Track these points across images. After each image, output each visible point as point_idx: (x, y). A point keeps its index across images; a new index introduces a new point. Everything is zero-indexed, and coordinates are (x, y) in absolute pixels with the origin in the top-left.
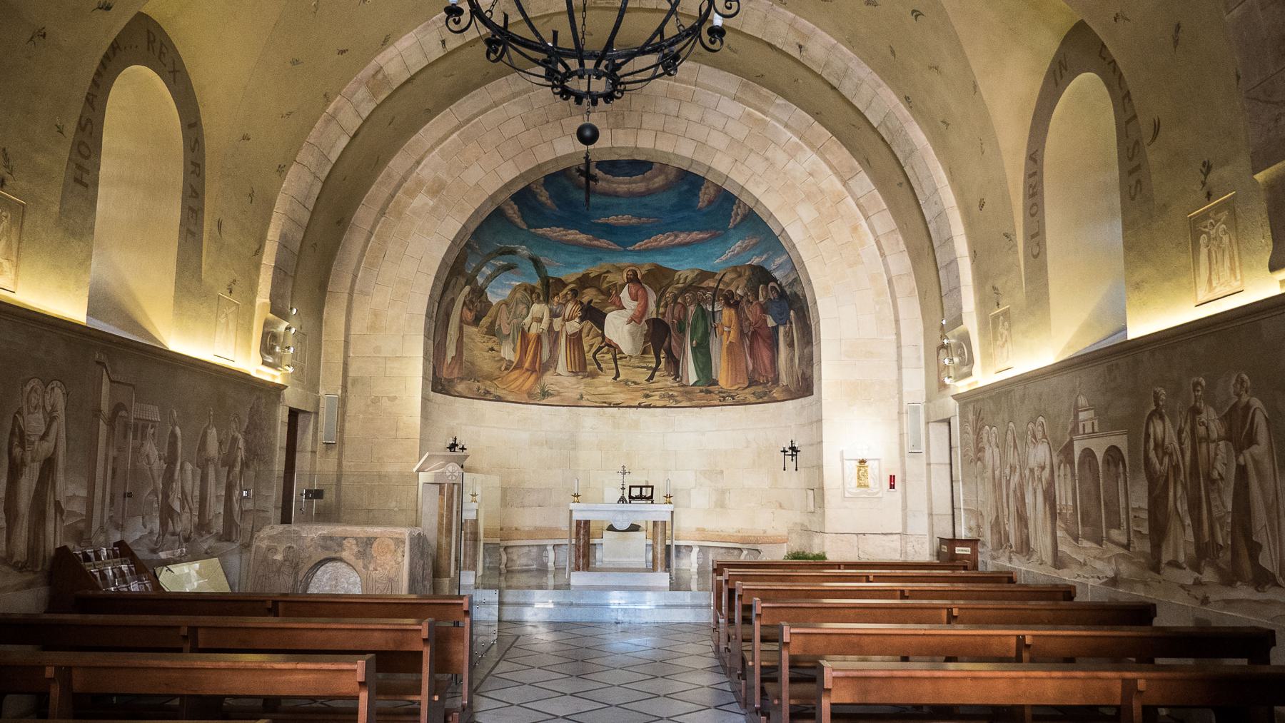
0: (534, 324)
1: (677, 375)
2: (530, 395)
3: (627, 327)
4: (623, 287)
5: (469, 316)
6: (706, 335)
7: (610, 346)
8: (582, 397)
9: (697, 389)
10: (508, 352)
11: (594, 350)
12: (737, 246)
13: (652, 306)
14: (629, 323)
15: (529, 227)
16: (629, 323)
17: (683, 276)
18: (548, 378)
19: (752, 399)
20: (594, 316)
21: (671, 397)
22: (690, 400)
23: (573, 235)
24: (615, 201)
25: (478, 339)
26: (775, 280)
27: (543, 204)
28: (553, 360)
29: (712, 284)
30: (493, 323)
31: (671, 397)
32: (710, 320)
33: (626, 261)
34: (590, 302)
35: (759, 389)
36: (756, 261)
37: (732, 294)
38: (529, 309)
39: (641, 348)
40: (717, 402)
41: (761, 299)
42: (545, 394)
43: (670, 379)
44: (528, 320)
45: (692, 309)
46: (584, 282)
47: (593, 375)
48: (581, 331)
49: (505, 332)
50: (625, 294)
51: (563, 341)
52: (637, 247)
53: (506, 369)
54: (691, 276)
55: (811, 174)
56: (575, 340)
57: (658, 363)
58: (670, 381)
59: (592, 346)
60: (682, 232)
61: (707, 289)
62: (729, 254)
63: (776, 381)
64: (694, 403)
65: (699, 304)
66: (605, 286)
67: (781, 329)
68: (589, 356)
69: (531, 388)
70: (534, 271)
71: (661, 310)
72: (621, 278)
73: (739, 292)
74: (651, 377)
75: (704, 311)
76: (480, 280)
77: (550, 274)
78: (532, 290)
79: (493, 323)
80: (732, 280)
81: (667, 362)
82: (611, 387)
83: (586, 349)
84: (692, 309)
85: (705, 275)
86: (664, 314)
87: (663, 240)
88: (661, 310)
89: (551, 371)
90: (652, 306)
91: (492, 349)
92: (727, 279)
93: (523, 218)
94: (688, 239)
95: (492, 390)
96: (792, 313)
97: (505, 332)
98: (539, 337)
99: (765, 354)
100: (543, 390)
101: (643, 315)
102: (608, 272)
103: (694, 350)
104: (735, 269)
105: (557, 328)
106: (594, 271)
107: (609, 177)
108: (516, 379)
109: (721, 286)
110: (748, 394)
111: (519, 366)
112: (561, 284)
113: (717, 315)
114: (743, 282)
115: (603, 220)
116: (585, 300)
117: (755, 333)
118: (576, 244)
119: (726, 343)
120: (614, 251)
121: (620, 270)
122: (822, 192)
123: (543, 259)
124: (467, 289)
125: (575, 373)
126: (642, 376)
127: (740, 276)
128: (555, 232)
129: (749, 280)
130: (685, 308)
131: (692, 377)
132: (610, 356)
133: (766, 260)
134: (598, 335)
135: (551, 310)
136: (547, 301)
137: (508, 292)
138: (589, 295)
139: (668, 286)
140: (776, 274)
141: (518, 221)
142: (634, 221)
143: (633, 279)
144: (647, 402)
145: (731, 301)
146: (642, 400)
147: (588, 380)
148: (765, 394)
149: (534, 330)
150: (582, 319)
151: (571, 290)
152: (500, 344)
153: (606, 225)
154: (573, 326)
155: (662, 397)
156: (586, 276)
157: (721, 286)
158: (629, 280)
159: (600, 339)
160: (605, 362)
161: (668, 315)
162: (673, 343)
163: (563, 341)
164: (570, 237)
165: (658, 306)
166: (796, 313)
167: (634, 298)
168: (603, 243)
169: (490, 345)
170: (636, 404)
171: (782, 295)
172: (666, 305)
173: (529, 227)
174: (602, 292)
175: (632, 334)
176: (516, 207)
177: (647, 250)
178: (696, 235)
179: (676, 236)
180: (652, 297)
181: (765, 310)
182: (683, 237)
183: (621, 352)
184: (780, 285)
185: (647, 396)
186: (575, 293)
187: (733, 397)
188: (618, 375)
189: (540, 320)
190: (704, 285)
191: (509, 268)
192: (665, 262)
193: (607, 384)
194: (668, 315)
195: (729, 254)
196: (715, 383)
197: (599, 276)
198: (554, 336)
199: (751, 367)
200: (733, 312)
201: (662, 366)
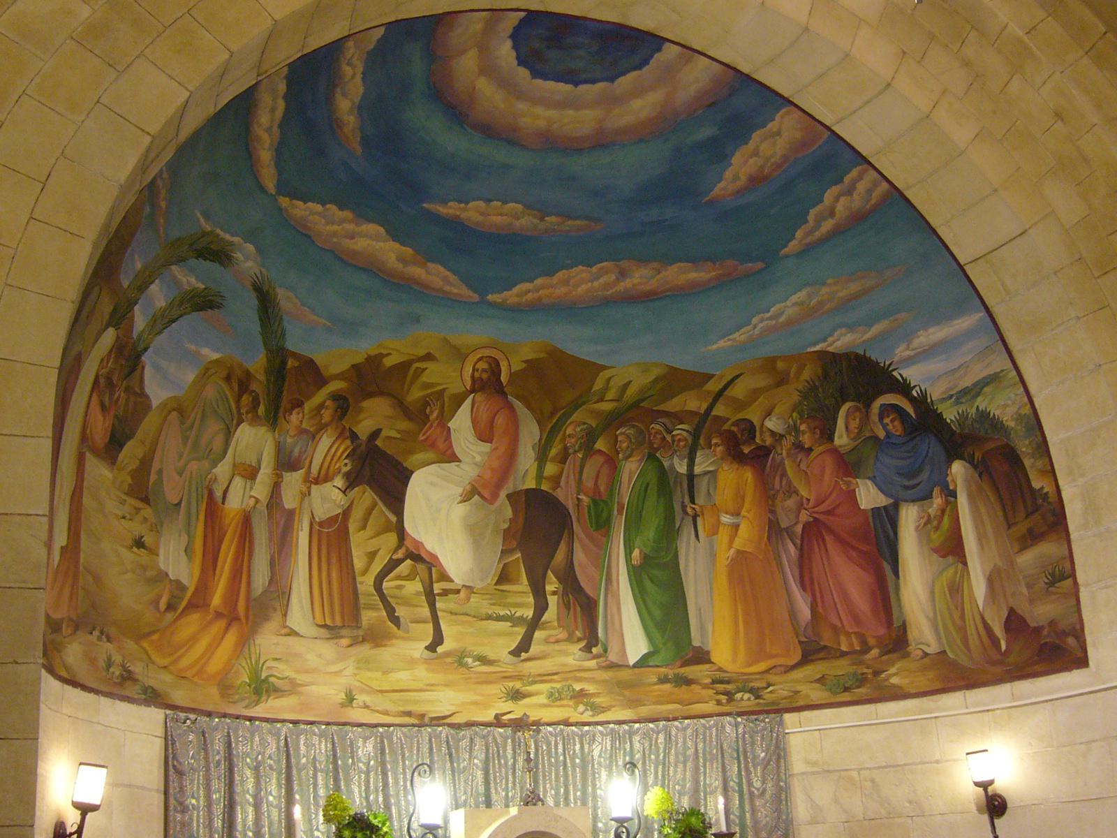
0: (238, 482)
1: (591, 640)
2: (226, 689)
3: (460, 510)
4: (458, 401)
5: (101, 427)
6: (669, 532)
7: (416, 557)
8: (350, 699)
9: (651, 676)
10: (176, 560)
11: (377, 567)
12: (788, 304)
13: (527, 459)
14: (466, 498)
15: (285, 188)
16: (466, 498)
17: (616, 383)
18: (268, 641)
19: (816, 693)
20: (382, 475)
21: (580, 696)
22: (633, 703)
23: (373, 241)
24: (500, 154)
25: (112, 506)
26: (904, 388)
27: (334, 124)
28: (279, 593)
29: (693, 402)
30: (145, 464)
31: (580, 696)
32: (680, 495)
33: (476, 334)
34: (376, 434)
35: (841, 668)
36: (842, 341)
37: (750, 429)
38: (229, 435)
39: (494, 570)
40: (710, 707)
41: (841, 439)
42: (262, 688)
43: (575, 649)
44: (223, 469)
45: (631, 468)
46: (371, 378)
47: (375, 638)
48: (346, 513)
49: (172, 497)
50: (461, 423)
51: (302, 538)
52: (511, 296)
53: (171, 607)
54: (640, 381)
55: (1058, 116)
56: (333, 537)
57: (541, 608)
58: (572, 656)
59: (372, 555)
60: (642, 260)
61: (678, 417)
62: (759, 323)
63: (897, 642)
64: (644, 711)
65: (652, 457)
66: (415, 394)
67: (909, 517)
68: (366, 584)
69: (227, 669)
70: (256, 328)
71: (550, 469)
72: (445, 376)
73: (772, 424)
74: (523, 647)
75: (663, 473)
76: (140, 321)
77: (291, 345)
78: (242, 383)
79: (145, 464)
80: (755, 394)
81: (566, 605)
82: (423, 674)
83: (358, 564)
84: (631, 468)
85: (676, 380)
86: (556, 480)
87: (583, 281)
88: (550, 469)
89: (273, 625)
90: (527, 459)
91: (139, 543)
92: (738, 391)
93: (279, 152)
94: (653, 284)
95: (137, 668)
96: (958, 469)
97: (172, 497)
98: (246, 521)
99: (849, 578)
100: (255, 673)
101: (499, 485)
102: (428, 357)
103: (637, 575)
104: (769, 364)
105: (289, 500)
106: (396, 350)
107: (523, 73)
108: (194, 639)
109: (720, 410)
110: (803, 681)
111: (199, 602)
112: (313, 374)
113: (702, 486)
114: (789, 397)
115: (450, 209)
116: (364, 428)
117: (814, 531)
118: (371, 268)
119: (725, 556)
120: (451, 302)
121: (460, 355)
122: (1085, 160)
123: (285, 299)
124: (109, 336)
125: (332, 631)
126: (500, 643)
127: (782, 381)
128: (326, 220)
129: (810, 392)
130: (612, 463)
131: (636, 644)
132: (414, 587)
133: (882, 336)
134: (386, 529)
135: (279, 449)
136: (273, 420)
137: (190, 376)
138: (375, 416)
139: (576, 405)
140: (912, 374)
141: (266, 156)
142: (526, 222)
143: (488, 383)
144: (516, 710)
145: (745, 447)
146: (504, 706)
147: (365, 650)
148: (862, 681)
149: (238, 499)
150: (353, 481)
151: (336, 397)
152: (156, 529)
153: (455, 225)
154: (329, 498)
155: (555, 698)
156: (374, 361)
157: (720, 410)
158: (478, 386)
159: (392, 538)
160: (407, 602)
161: (569, 480)
162: (579, 556)
163: (302, 538)
164: (361, 244)
165: (542, 458)
166: (982, 468)
167: (484, 433)
168: (435, 275)
169: (137, 528)
170: (489, 716)
171: (924, 421)
172: (563, 458)
173: (285, 188)
174: (405, 411)
175: (474, 531)
176: (281, 105)
177: (537, 308)
178: (679, 274)
179: (623, 274)
180: (530, 433)
181: (849, 466)
182: (640, 278)
183: (445, 577)
184: (921, 403)
185: (516, 696)
186: (343, 406)
187: (756, 692)
188: (438, 639)
189: (251, 473)
190: (674, 405)
191: (204, 302)
192: (576, 341)
193: (412, 663)
194: (569, 480)
195: (759, 323)
196: (701, 657)
197: (404, 366)
198: (283, 523)
199: (805, 612)
200: (748, 475)
201: (551, 614)
